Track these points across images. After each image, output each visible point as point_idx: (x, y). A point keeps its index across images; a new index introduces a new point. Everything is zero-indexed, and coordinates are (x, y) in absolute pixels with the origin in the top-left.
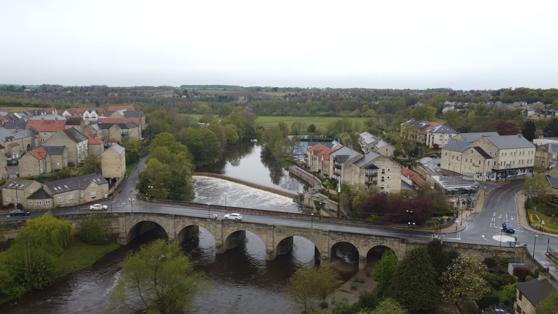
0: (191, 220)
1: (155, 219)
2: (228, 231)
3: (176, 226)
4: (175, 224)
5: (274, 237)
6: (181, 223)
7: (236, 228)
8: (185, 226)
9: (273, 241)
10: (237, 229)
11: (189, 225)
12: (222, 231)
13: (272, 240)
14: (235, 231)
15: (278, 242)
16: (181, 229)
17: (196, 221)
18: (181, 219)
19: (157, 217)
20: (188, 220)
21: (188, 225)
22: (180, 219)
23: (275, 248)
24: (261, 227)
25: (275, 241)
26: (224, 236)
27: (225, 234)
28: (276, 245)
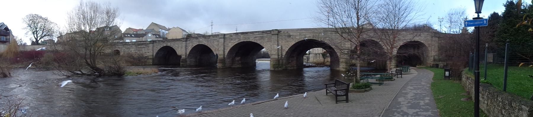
0: (198, 40)
2: (230, 44)
3: (187, 47)
4: (186, 46)
6: (191, 44)
8: (193, 46)
11: (196, 44)
12: (224, 46)
14: (236, 43)
16: (190, 49)
20: (196, 40)
21: (195, 45)
24: (265, 35)
26: (225, 50)
27: (226, 48)
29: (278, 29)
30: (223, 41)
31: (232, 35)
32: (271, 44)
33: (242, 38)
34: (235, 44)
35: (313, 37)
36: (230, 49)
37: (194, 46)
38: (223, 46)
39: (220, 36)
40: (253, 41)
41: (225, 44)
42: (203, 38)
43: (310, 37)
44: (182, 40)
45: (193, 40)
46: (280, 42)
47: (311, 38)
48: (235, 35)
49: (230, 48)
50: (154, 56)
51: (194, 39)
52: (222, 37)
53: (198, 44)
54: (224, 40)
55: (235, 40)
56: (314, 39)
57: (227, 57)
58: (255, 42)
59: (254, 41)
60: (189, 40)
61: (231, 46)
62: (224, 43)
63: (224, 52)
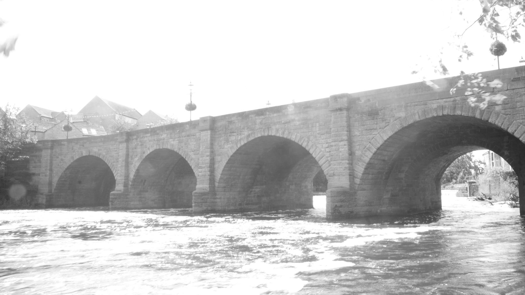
0: (155, 137)
1: (99, 150)
3: (130, 159)
4: (127, 155)
5: (355, 139)
6: (139, 150)
7: (246, 133)
9: (351, 154)
10: (249, 136)
11: (151, 150)
13: (344, 149)
14: (242, 143)
15: (368, 156)
17: (164, 136)
18: (139, 139)
23: (358, 181)
25: (358, 153)
26: (216, 166)
28: (360, 169)
29: (350, 92)
30: (209, 139)
31: (233, 119)
32: (329, 140)
33: (257, 126)
34: (239, 146)
35: (455, 108)
36: (226, 162)
37: (146, 154)
38: (208, 154)
39: (201, 125)
40: (280, 134)
41: (216, 147)
42: (168, 132)
43: (443, 108)
44: (117, 139)
45: (146, 139)
46: (357, 133)
47: (445, 113)
48: (240, 118)
49: (228, 159)
50: (55, 184)
51: (149, 135)
52: (207, 125)
53: (155, 147)
54: (211, 134)
55: (240, 134)
56: (458, 113)
57: (222, 185)
58: (285, 136)
59: (281, 136)
60: (136, 139)
61: (231, 152)
62: (212, 144)
63: (212, 170)
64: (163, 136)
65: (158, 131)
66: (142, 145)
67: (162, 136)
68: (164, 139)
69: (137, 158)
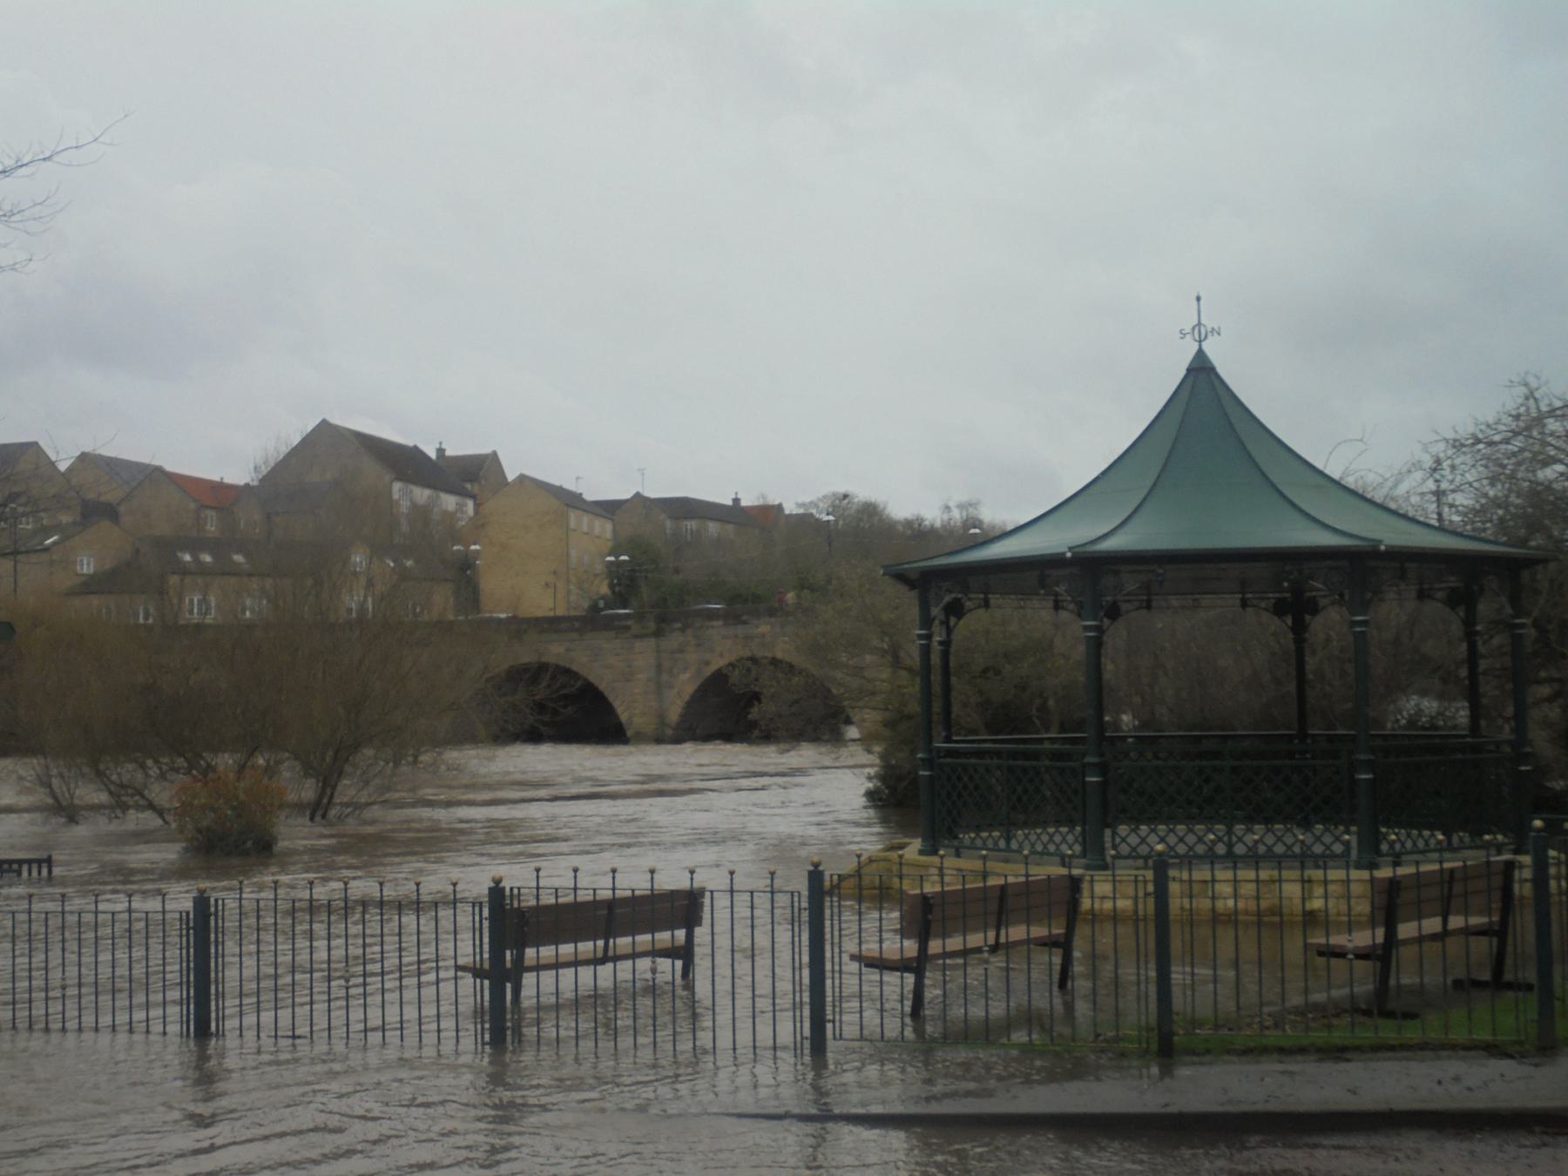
1: (568, 650)
3: (665, 677)
4: (659, 667)
18: (689, 631)
19: (574, 635)
22: (683, 630)
42: (773, 620)
44: (627, 628)
51: (720, 623)
60: (683, 630)
64: (760, 630)
65: (745, 618)
66: (698, 645)
67: (757, 627)
68: (763, 636)
69: (687, 675)
